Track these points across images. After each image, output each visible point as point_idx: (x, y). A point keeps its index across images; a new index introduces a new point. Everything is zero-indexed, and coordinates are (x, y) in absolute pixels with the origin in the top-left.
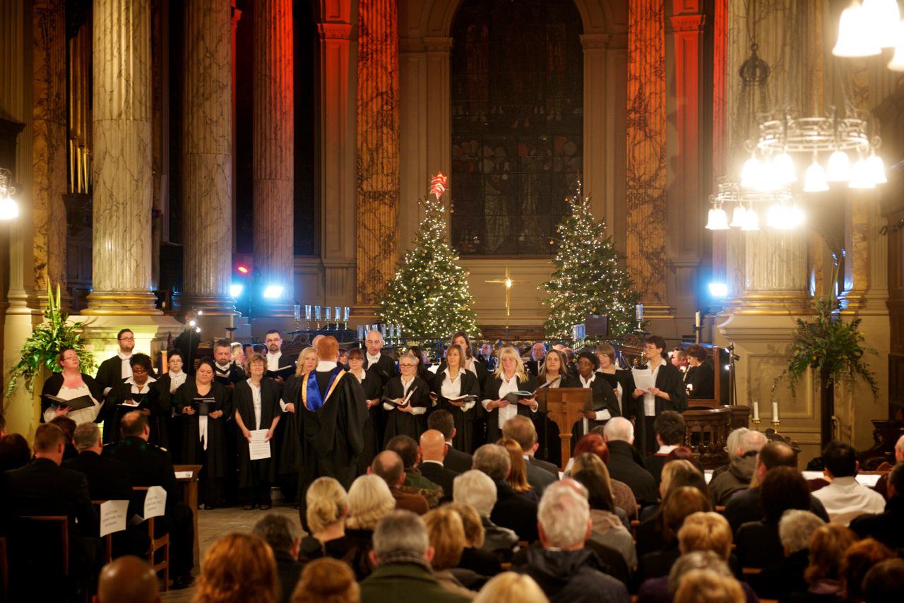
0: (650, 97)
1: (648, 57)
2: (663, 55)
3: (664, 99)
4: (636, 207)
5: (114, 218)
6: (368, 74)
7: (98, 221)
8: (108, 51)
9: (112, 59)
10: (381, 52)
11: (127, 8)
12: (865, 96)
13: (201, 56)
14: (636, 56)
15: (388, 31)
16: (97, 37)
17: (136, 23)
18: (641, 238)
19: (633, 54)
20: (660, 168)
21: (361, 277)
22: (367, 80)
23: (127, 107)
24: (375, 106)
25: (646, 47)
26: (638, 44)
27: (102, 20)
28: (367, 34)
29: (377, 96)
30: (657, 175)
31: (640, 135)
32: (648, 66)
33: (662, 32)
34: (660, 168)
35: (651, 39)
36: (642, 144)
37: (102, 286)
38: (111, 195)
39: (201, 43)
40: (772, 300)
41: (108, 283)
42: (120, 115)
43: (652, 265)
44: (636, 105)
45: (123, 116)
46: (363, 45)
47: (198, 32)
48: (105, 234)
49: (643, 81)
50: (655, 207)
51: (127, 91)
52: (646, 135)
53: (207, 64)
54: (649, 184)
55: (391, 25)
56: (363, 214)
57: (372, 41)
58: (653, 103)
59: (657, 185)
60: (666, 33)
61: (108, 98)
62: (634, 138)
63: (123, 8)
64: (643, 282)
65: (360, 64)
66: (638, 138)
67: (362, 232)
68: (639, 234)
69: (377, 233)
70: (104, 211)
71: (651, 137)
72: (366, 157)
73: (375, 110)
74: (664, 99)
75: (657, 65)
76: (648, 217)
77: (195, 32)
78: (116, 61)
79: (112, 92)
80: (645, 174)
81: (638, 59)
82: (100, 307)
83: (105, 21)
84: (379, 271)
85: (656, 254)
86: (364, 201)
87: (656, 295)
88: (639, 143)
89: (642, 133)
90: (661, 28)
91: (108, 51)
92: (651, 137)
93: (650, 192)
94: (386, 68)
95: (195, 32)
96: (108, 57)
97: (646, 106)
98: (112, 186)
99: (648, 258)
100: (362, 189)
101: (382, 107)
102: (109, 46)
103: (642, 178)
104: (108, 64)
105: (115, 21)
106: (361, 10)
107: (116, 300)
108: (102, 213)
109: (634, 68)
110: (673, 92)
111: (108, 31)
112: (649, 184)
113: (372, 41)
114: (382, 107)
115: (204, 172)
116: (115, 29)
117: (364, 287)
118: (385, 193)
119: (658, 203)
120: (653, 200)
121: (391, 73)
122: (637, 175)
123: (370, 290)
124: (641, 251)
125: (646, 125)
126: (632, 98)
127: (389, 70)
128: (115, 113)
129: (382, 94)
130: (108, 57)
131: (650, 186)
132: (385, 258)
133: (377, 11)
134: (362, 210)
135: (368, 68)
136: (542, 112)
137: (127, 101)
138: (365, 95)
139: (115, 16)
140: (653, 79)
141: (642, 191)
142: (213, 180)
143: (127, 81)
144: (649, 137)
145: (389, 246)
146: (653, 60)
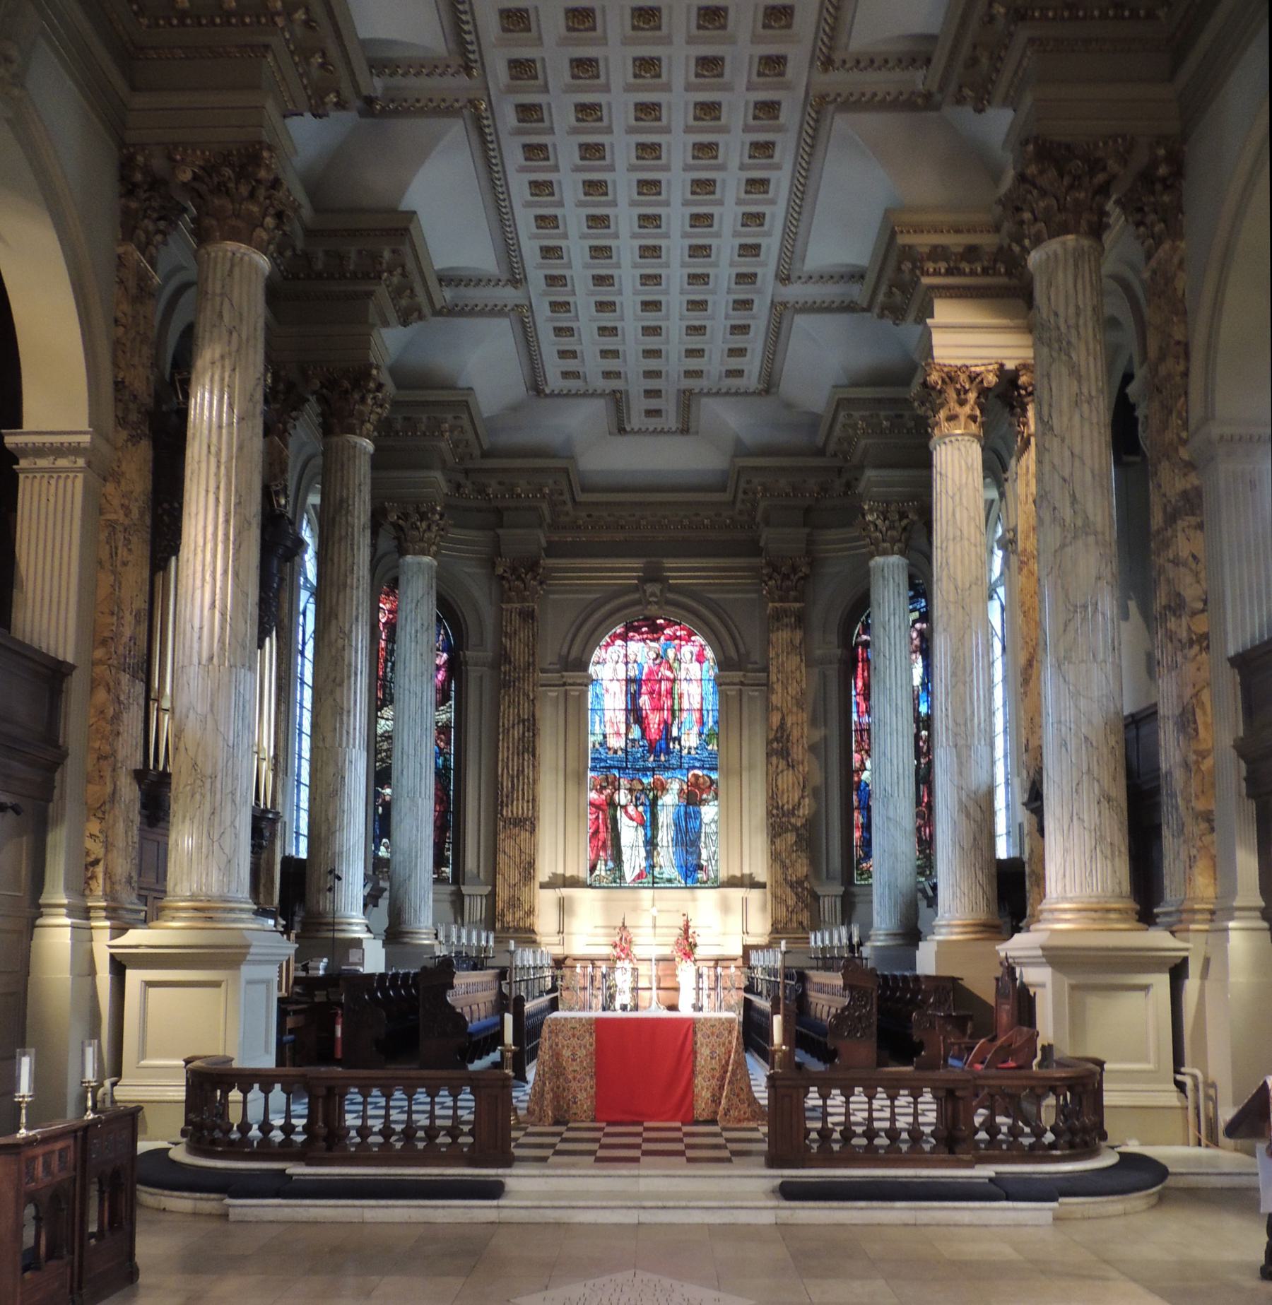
0: (792, 728)
1: (790, 689)
2: (804, 686)
3: (806, 730)
4: (780, 835)
5: (198, 797)
6: (509, 702)
7: (176, 801)
8: (199, 575)
9: (203, 586)
10: (524, 680)
11: (227, 521)
12: (1204, 644)
13: (333, 637)
14: (778, 687)
15: (531, 660)
16: (185, 559)
17: (237, 543)
18: (784, 866)
19: (775, 686)
20: (803, 797)
21: (500, 905)
22: (509, 707)
23: (222, 648)
24: (516, 733)
25: (788, 679)
26: (780, 677)
27: (192, 537)
28: (510, 662)
29: (518, 723)
30: (799, 804)
31: (782, 764)
32: (789, 698)
33: (803, 665)
34: (803, 797)
35: (792, 672)
36: (785, 773)
37: (178, 889)
38: (195, 765)
39: (334, 622)
40: (1095, 911)
41: (186, 885)
42: (211, 658)
43: (797, 894)
44: (779, 735)
45: (215, 660)
46: (505, 673)
47: (331, 608)
48: (184, 817)
49: (784, 710)
50: (798, 835)
51: (222, 628)
52: (788, 765)
53: (340, 646)
54: (792, 813)
55: (533, 654)
56: (504, 840)
57: (515, 669)
58: (796, 733)
59: (801, 814)
60: (806, 666)
61: (196, 636)
62: (777, 767)
63: (221, 519)
64: (787, 910)
65: (502, 691)
66: (780, 768)
67: (501, 858)
68: (781, 861)
69: (518, 860)
70: (185, 786)
71: (793, 767)
72: (507, 784)
73: (516, 737)
74: (806, 730)
75: (799, 697)
76: (792, 846)
77: (328, 610)
78: (208, 588)
79: (201, 628)
80: (788, 802)
81: (780, 691)
82: (173, 919)
83: (196, 536)
84: (519, 899)
85: (800, 883)
86: (504, 827)
87: (801, 923)
88: (782, 771)
89: (785, 762)
90: (801, 660)
91: (199, 575)
92: (793, 767)
93: (793, 820)
94: (528, 696)
95: (328, 610)
96: (198, 583)
97: (788, 736)
98: (197, 751)
99: (791, 887)
100: (502, 815)
101: (524, 733)
102: (199, 568)
103: (786, 807)
104: (198, 593)
105: (209, 536)
106: (504, 639)
107: (196, 909)
108: (181, 788)
109: (776, 699)
110: (813, 722)
111: (199, 550)
112: (792, 813)
113: (515, 669)
114: (524, 733)
115: (331, 770)
116: (209, 546)
117: (503, 916)
118: (526, 820)
119: (802, 831)
120: (795, 828)
121: (533, 700)
122: (780, 804)
123: (509, 918)
124: (785, 879)
125: (788, 754)
126: (775, 728)
127: (531, 697)
128: (205, 655)
129: (524, 721)
130: (198, 583)
131: (793, 814)
132: (525, 885)
133: (520, 640)
134: (502, 836)
135: (509, 696)
136: (677, 747)
137: (221, 640)
138: (506, 722)
139: (210, 529)
140: (795, 709)
141: (783, 820)
142: (343, 778)
143: (223, 614)
144: (791, 766)
145: (530, 873)
146: (794, 692)
